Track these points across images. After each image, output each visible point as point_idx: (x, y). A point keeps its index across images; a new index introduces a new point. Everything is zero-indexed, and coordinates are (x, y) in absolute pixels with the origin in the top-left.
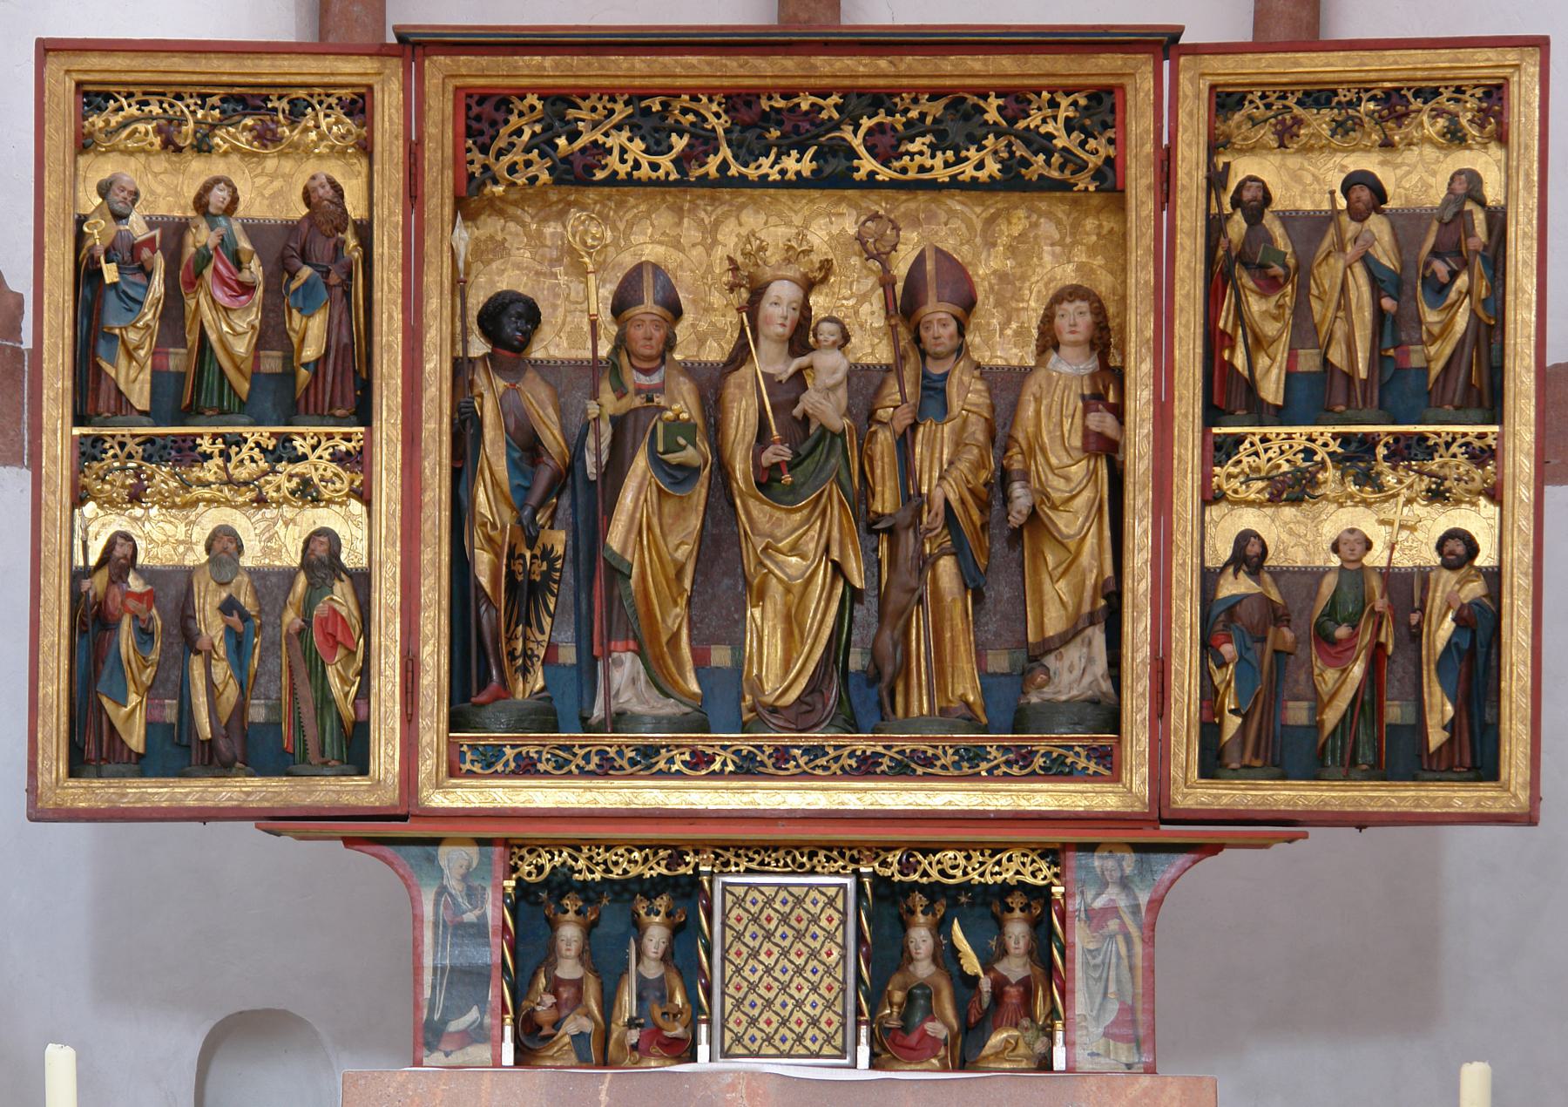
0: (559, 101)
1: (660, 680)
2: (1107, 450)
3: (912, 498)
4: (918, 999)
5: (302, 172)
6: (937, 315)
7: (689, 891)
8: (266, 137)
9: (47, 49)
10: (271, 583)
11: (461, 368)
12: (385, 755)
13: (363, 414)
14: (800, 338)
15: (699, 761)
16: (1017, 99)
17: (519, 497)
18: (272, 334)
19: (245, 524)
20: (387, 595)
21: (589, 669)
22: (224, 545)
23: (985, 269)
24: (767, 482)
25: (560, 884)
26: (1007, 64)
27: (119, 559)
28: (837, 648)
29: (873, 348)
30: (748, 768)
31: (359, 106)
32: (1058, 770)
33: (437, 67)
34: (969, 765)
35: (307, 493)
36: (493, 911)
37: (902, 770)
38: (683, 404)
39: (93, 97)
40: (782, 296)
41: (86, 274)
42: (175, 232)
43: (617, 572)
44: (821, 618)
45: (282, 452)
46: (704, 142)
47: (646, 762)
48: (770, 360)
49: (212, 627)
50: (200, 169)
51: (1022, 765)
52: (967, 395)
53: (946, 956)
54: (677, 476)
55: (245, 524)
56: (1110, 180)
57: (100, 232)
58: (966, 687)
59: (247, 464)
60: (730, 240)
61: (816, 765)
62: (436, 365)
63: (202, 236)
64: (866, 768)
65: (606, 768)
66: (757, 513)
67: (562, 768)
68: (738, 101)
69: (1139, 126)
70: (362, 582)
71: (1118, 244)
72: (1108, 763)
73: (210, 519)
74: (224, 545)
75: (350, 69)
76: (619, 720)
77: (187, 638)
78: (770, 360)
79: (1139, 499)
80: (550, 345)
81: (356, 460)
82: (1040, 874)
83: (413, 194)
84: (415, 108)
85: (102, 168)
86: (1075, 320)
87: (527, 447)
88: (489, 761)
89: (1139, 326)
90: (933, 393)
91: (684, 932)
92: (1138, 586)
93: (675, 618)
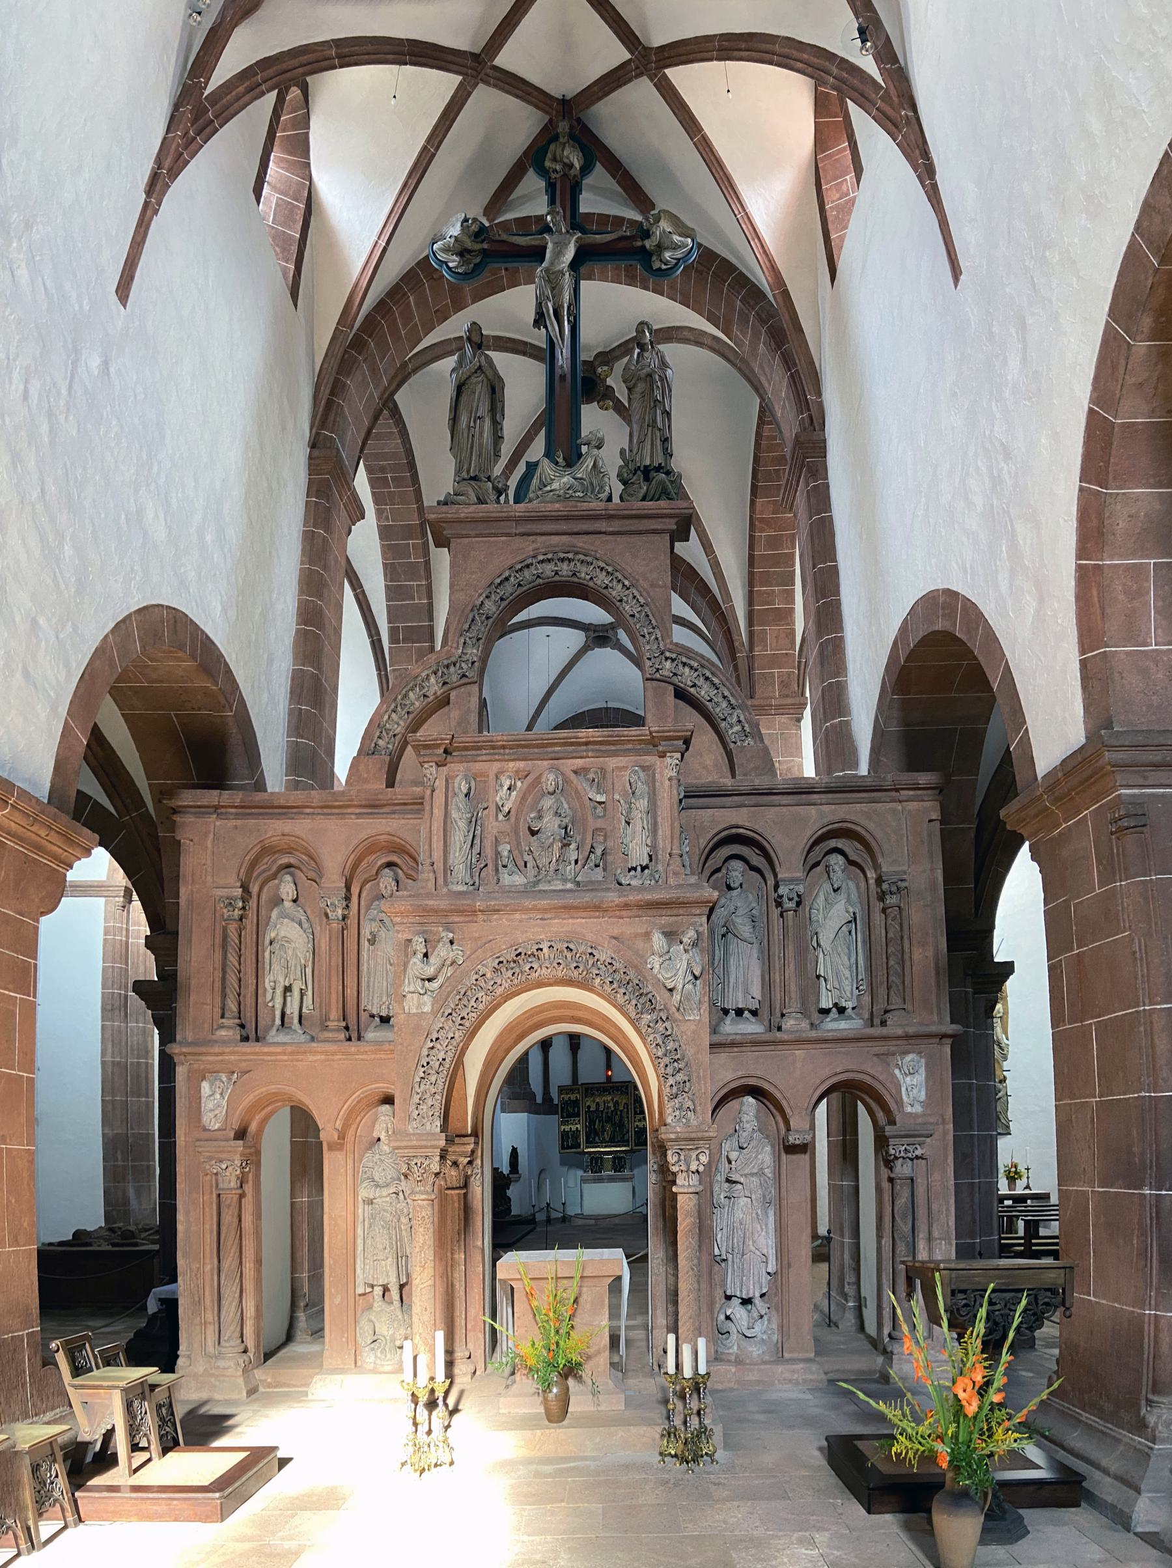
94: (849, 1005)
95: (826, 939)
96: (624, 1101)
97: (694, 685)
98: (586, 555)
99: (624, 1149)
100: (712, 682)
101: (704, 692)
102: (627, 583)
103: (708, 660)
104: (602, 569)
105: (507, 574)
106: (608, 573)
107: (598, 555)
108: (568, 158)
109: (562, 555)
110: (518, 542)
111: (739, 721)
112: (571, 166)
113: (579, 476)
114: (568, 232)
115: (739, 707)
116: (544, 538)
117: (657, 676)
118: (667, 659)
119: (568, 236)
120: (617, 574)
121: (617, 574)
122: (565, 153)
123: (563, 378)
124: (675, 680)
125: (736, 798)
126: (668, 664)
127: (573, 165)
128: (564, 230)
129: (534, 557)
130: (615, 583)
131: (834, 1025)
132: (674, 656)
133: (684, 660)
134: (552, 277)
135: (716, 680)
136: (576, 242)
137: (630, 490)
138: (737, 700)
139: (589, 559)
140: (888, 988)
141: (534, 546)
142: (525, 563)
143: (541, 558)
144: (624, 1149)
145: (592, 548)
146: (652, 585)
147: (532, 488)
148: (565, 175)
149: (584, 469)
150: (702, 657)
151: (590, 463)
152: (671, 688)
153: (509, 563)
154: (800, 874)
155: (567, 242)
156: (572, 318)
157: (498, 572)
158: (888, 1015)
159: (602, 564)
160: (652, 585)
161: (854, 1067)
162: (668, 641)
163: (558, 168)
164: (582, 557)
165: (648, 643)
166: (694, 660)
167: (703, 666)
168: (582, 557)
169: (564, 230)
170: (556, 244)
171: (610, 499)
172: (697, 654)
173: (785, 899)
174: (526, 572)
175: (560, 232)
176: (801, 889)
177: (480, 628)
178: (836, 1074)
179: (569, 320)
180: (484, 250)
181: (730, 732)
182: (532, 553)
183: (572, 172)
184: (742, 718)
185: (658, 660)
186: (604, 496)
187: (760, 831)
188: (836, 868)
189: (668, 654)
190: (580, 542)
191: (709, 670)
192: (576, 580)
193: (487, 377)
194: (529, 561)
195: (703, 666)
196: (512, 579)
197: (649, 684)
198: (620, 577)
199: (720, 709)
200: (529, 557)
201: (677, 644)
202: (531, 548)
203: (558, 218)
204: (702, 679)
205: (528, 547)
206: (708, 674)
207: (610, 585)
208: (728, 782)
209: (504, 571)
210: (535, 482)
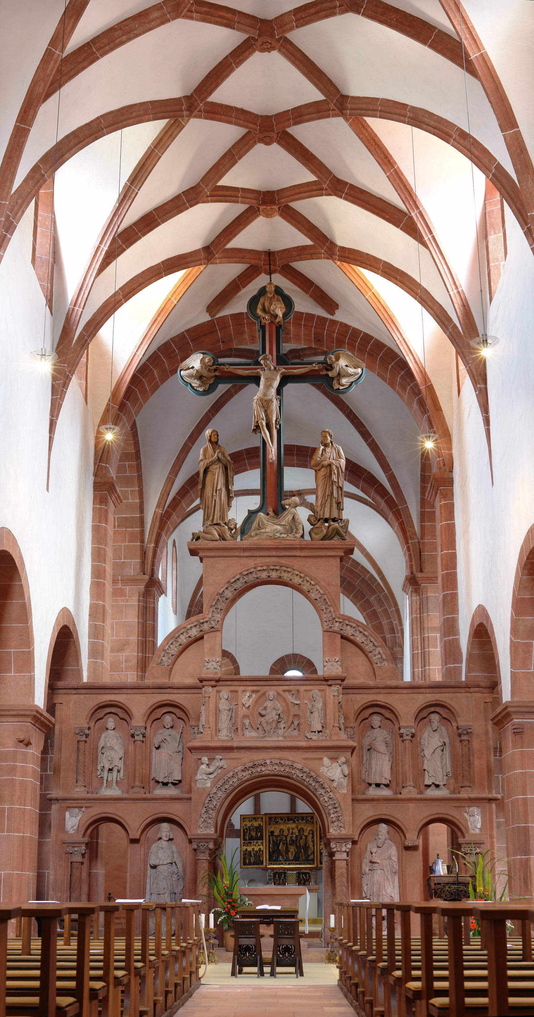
0: (275, 818)
1: (283, 858)
2: (313, 841)
3: (300, 845)
4: (301, 880)
5: (258, 823)
6: (302, 832)
7: (285, 873)
8: (256, 821)
9: (241, 815)
10: (257, 851)
11: (269, 836)
12: (264, 864)
13: (262, 840)
14: (292, 834)
15: (286, 864)
16: (307, 817)
17: (273, 845)
18: (256, 834)
19: (255, 848)
20: (264, 852)
21: (278, 857)
22: (253, 849)
23: (305, 828)
24: (290, 844)
25: (276, 872)
26: (306, 815)
27: (246, 850)
28: (295, 855)
29: (297, 834)
30: (289, 864)
31: (262, 818)
32: (310, 864)
33: (267, 816)
34: (304, 864)
35: (259, 845)
36: (272, 874)
37: (300, 864)
38: (284, 839)
39: (244, 818)
40: (291, 831)
41: (244, 830)
42: (250, 827)
43: (280, 850)
44: (294, 853)
45: (257, 842)
46: (285, 820)
47: (282, 864)
48: (290, 835)
49: (253, 855)
50: (251, 823)
51: (308, 864)
52: (304, 837)
53: (303, 877)
54: (284, 844)
55: (255, 848)
56: (313, 822)
57: (245, 827)
58: (304, 858)
59: (255, 843)
60: (287, 826)
61: (294, 864)
62: (267, 836)
63: (252, 828)
64: (297, 864)
65: (279, 864)
66: (289, 846)
67: (276, 864)
68: (288, 817)
69: (315, 819)
70: (263, 851)
71: (313, 826)
72: (314, 864)
73: (252, 847)
74: (253, 849)
75: (261, 816)
76: (280, 861)
77: (251, 856)
78: (290, 835)
79: (315, 845)
80: (275, 834)
81: (262, 843)
82: (309, 871)
83: (266, 824)
84: (266, 818)
85: (245, 823)
86: (311, 832)
87: (273, 841)
88: (271, 864)
89: (315, 833)
90: (301, 838)
91: (285, 876)
92: (315, 851)
93: (284, 853)
94: (441, 784)
95: (427, 752)
96: (309, 828)
97: (353, 635)
98: (287, 568)
99: (309, 866)
100: (364, 634)
101: (359, 639)
102: (313, 583)
103: (362, 623)
104: (297, 575)
105: (238, 577)
106: (301, 577)
107: (295, 568)
108: (273, 311)
109: (272, 567)
110: (244, 561)
111: (380, 653)
112: (276, 316)
113: (284, 524)
114: (275, 368)
115: (379, 646)
116: (261, 558)
117: (331, 630)
118: (336, 622)
119: (275, 372)
120: (307, 578)
121: (307, 578)
122: (272, 308)
123: (272, 464)
124: (342, 632)
125: (376, 690)
126: (337, 624)
127: (277, 315)
128: (272, 368)
129: (255, 568)
130: (305, 582)
131: (432, 793)
132: (341, 620)
133: (347, 622)
134: (265, 403)
135: (366, 633)
136: (281, 374)
137: (315, 531)
138: (378, 643)
139: (289, 570)
140: (463, 776)
141: (255, 562)
142: (249, 571)
143: (259, 568)
144: (309, 866)
145: (291, 564)
146: (328, 584)
147: (253, 528)
148: (272, 322)
149: (286, 518)
150: (358, 621)
151: (290, 517)
152: (339, 636)
153: (239, 572)
154: (412, 724)
155: (274, 377)
156: (278, 427)
157: (232, 576)
158: (463, 789)
159: (298, 573)
160: (328, 584)
161: (442, 812)
162: (338, 613)
163: (267, 318)
164: (284, 568)
165: (326, 613)
166: (354, 623)
167: (358, 626)
168: (284, 568)
169: (272, 368)
170: (267, 379)
171: (302, 536)
172: (355, 620)
173: (404, 735)
174: (250, 576)
175: (270, 369)
176: (413, 731)
177: (222, 605)
178: (432, 815)
179: (276, 427)
180: (216, 376)
181: (374, 658)
182: (253, 566)
183: (277, 320)
184: (381, 652)
185: (331, 622)
186: (298, 535)
187: (390, 703)
188: (434, 721)
189: (337, 620)
190: (283, 561)
191: (362, 628)
192: (281, 580)
193: (222, 463)
194: (252, 570)
195: (358, 626)
196: (241, 579)
197: (325, 633)
198: (309, 579)
199: (368, 647)
200: (252, 568)
201: (343, 615)
202: (252, 564)
203: (268, 362)
204: (358, 632)
205: (251, 563)
206: (362, 630)
207: (302, 583)
208: (371, 683)
209: (237, 575)
210: (255, 525)
